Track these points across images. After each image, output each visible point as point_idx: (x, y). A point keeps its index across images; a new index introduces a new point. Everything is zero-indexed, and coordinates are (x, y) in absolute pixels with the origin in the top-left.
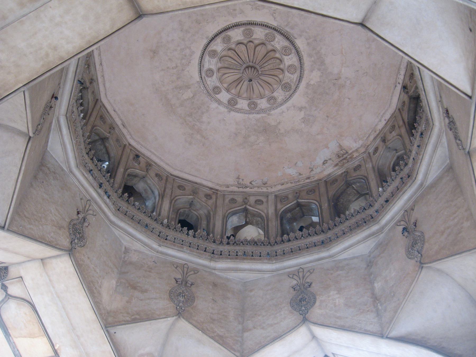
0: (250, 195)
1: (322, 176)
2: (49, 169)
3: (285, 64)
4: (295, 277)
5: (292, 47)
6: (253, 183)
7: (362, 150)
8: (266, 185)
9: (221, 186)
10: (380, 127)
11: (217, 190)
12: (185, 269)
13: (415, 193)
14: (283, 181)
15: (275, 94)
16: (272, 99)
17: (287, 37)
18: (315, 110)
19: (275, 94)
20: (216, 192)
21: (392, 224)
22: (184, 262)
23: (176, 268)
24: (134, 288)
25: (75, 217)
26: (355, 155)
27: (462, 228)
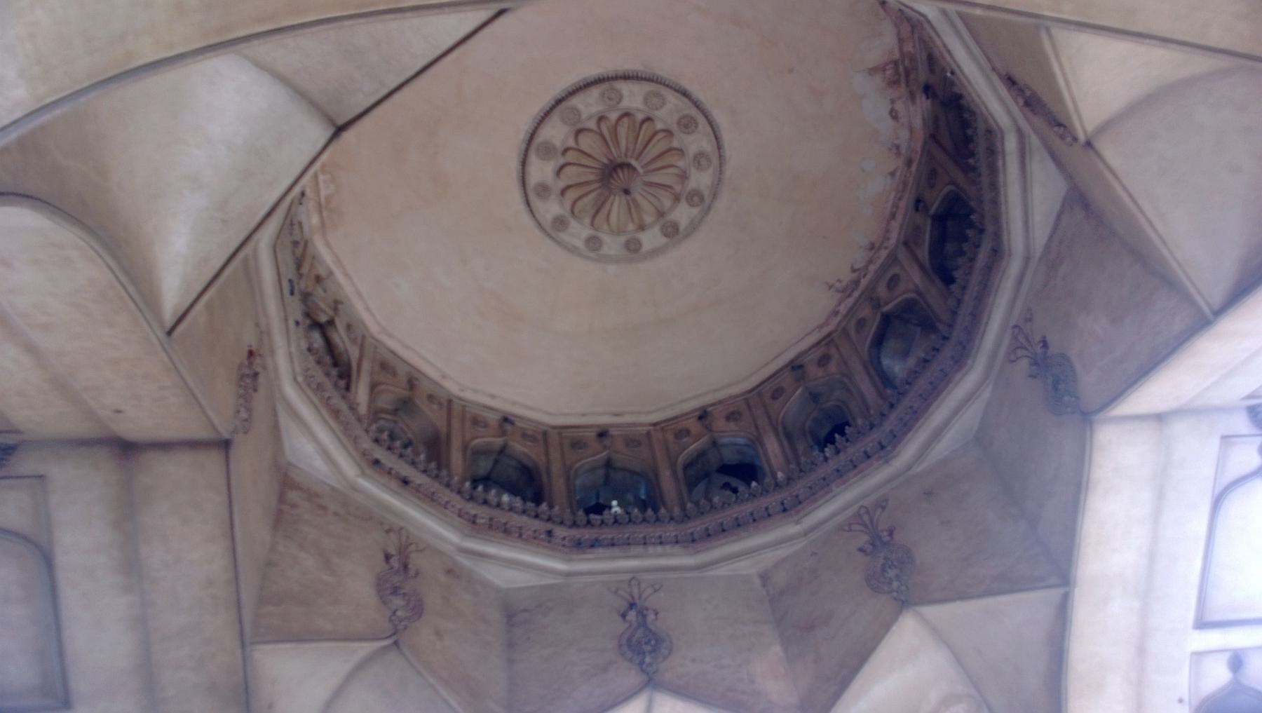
0: (871, 288)
2: (526, 610)
3: (638, 110)
4: (1020, 352)
6: (856, 267)
8: (877, 245)
9: (826, 323)
11: (829, 335)
12: (866, 518)
15: (692, 150)
19: (692, 150)
20: (828, 340)
22: (855, 508)
23: (850, 530)
24: (810, 628)
25: (621, 627)
26: (908, 48)
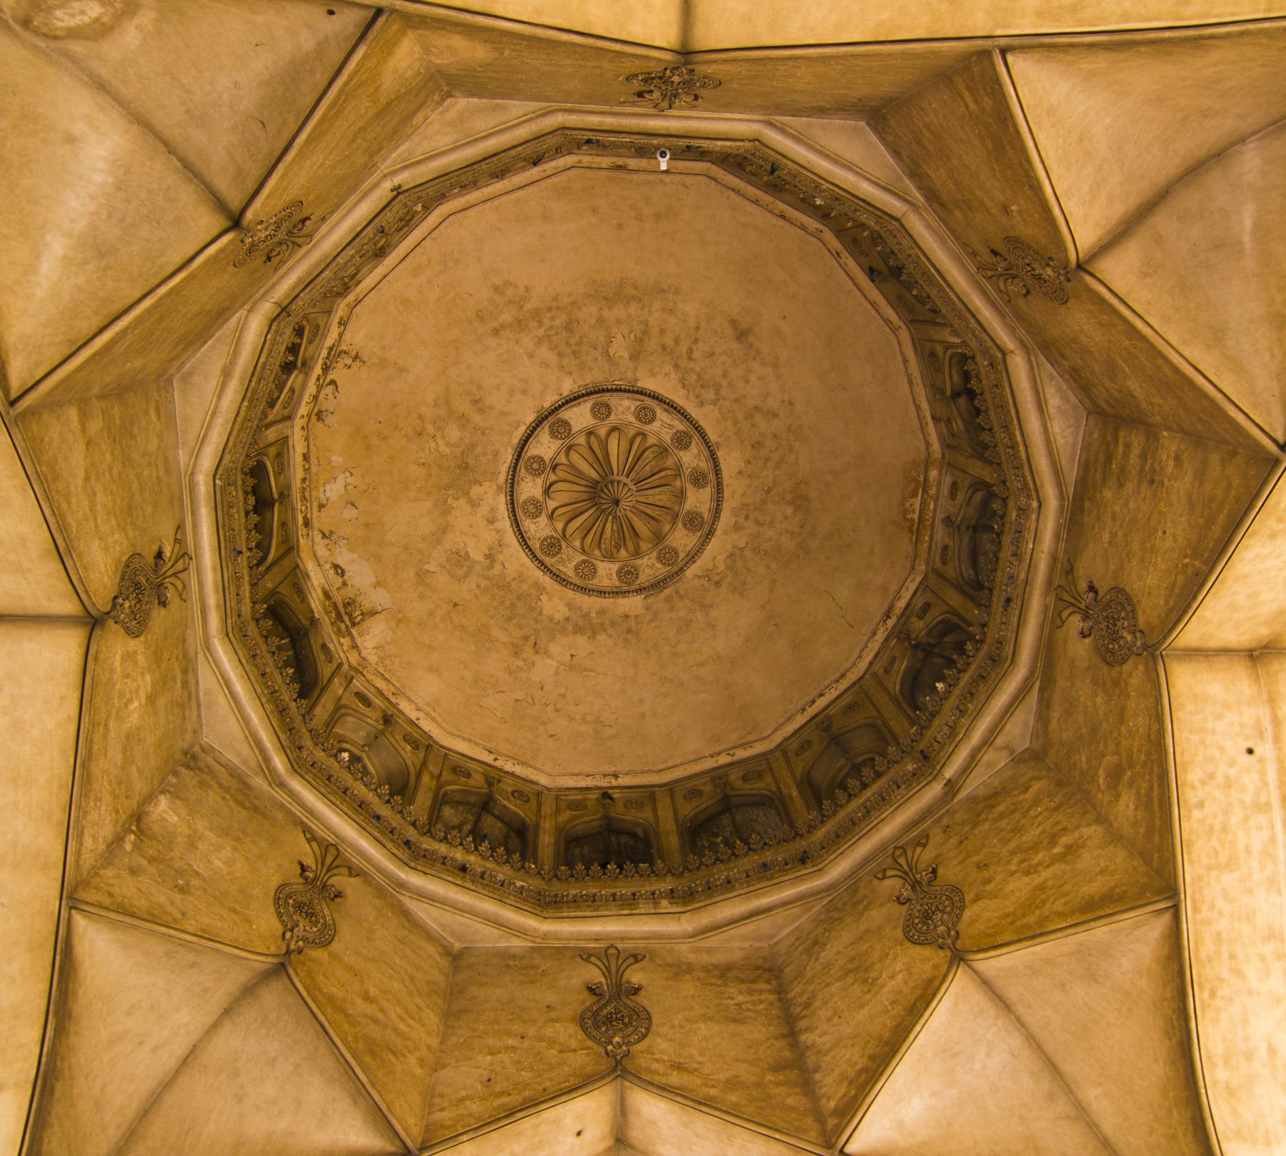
1: (305, 555)
5: (633, 587)
6: (330, 389)
7: (354, 659)
8: (314, 418)
10: (405, 706)
13: (381, 870)
14: (313, 461)
15: (543, 520)
16: (536, 508)
17: (657, 585)
18: (478, 586)
19: (543, 520)
21: (296, 810)
26: (346, 641)
27: (404, 1055)
